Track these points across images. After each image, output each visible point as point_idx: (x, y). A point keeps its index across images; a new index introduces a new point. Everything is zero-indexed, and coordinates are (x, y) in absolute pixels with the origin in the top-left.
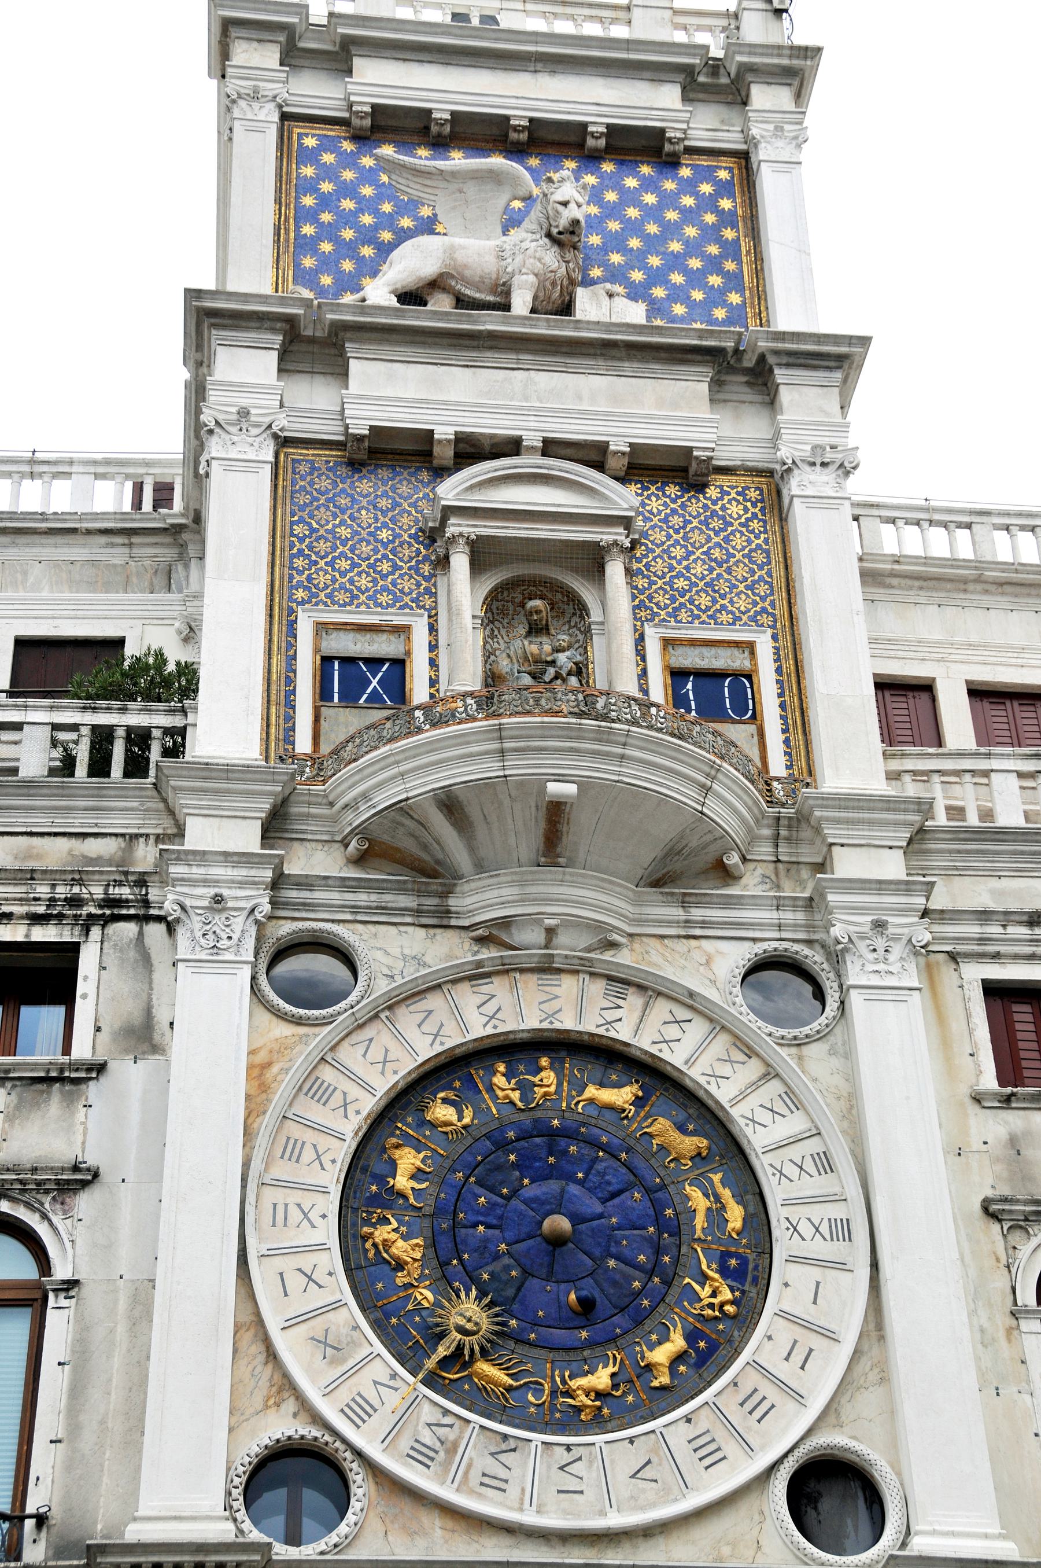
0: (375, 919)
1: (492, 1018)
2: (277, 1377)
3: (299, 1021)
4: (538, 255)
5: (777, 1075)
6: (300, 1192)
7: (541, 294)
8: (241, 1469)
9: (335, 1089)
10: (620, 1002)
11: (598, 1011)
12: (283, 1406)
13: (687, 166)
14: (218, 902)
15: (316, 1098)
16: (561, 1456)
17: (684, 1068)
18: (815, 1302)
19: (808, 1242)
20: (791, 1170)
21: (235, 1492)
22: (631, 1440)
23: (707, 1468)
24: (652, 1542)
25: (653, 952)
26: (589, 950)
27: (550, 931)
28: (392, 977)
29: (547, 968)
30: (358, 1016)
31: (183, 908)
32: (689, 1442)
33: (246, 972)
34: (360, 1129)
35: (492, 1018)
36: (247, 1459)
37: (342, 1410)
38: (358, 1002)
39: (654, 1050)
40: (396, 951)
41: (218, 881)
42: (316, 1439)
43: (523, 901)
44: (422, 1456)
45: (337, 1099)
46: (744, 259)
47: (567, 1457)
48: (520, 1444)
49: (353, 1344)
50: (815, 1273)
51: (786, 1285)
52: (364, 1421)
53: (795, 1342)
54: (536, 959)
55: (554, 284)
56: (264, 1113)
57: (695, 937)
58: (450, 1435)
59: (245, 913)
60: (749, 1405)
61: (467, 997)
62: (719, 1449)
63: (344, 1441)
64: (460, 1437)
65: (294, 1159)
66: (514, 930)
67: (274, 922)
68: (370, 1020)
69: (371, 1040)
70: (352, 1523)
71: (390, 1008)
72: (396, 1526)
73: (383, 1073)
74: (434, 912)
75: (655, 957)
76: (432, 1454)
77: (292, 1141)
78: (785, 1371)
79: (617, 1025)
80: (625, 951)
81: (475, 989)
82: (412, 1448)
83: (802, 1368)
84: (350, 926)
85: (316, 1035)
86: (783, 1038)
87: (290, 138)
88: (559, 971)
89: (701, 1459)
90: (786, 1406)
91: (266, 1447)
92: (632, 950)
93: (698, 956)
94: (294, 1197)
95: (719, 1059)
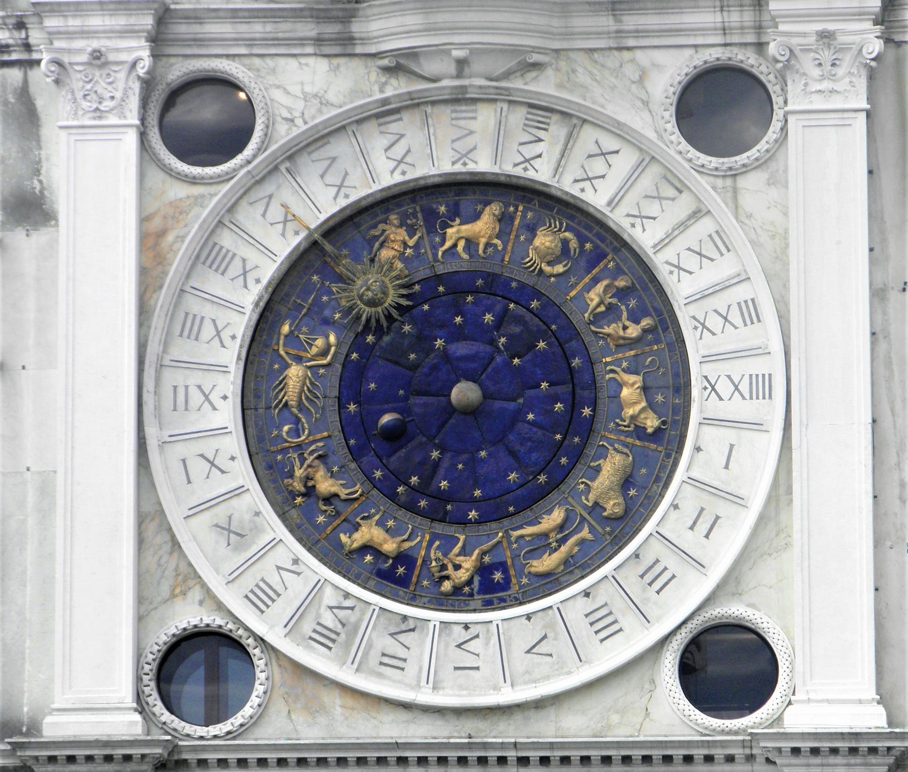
0: (273, 51)
1: (400, 162)
2: (183, 567)
3: (194, 181)
5: (709, 212)
6: (200, 373)
8: (151, 657)
9: (234, 255)
10: (541, 134)
11: (515, 146)
12: (190, 595)
14: (98, 58)
15: (214, 266)
16: (459, 634)
17: (606, 211)
18: (727, 467)
19: (726, 402)
20: (714, 322)
21: (146, 678)
22: (528, 617)
23: (602, 641)
24: (543, 713)
25: (580, 70)
26: (506, 75)
27: (461, 63)
28: (292, 121)
29: (460, 99)
30: (254, 173)
31: (59, 64)
32: (587, 616)
33: (131, 139)
34: (260, 299)
35: (400, 162)
36: (156, 648)
37: (246, 597)
38: (255, 156)
39: (575, 190)
40: (296, 90)
41: (96, 32)
42: (220, 627)
43: (429, 29)
44: (325, 638)
45: (236, 268)
47: (466, 635)
48: (419, 624)
49: (257, 530)
50: (730, 435)
51: (698, 449)
52: (268, 606)
53: (702, 510)
54: (448, 91)
56: (161, 287)
57: (629, 49)
58: (352, 617)
59: (127, 67)
60: (649, 577)
61: (376, 141)
62: (615, 622)
63: (247, 629)
64: (360, 620)
65: (193, 337)
66: (422, 60)
67: (165, 59)
68: (270, 173)
69: (270, 197)
70: (256, 705)
71: (290, 158)
72: (299, 706)
73: (283, 235)
74: (336, 40)
75: (582, 77)
76: (333, 636)
77: (190, 317)
78: (690, 541)
79: (537, 163)
80: (550, 72)
81: (383, 128)
82: (315, 631)
83: (707, 536)
84: (247, 61)
85: (216, 194)
86: (717, 169)
88: (474, 101)
89: (596, 632)
90: (689, 574)
91: (174, 635)
92: (558, 70)
93: (631, 72)
94: (195, 378)
95: (646, 197)
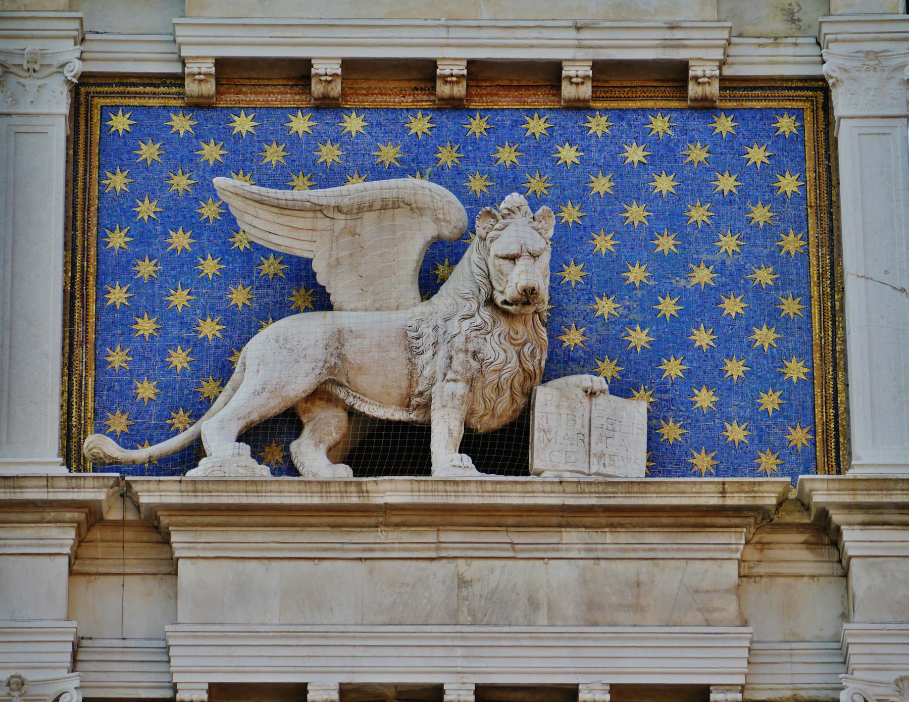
4: (471, 347)
7: (480, 409)
13: (728, 112)
46: (815, 294)
55: (498, 388)
87: (88, 119)
